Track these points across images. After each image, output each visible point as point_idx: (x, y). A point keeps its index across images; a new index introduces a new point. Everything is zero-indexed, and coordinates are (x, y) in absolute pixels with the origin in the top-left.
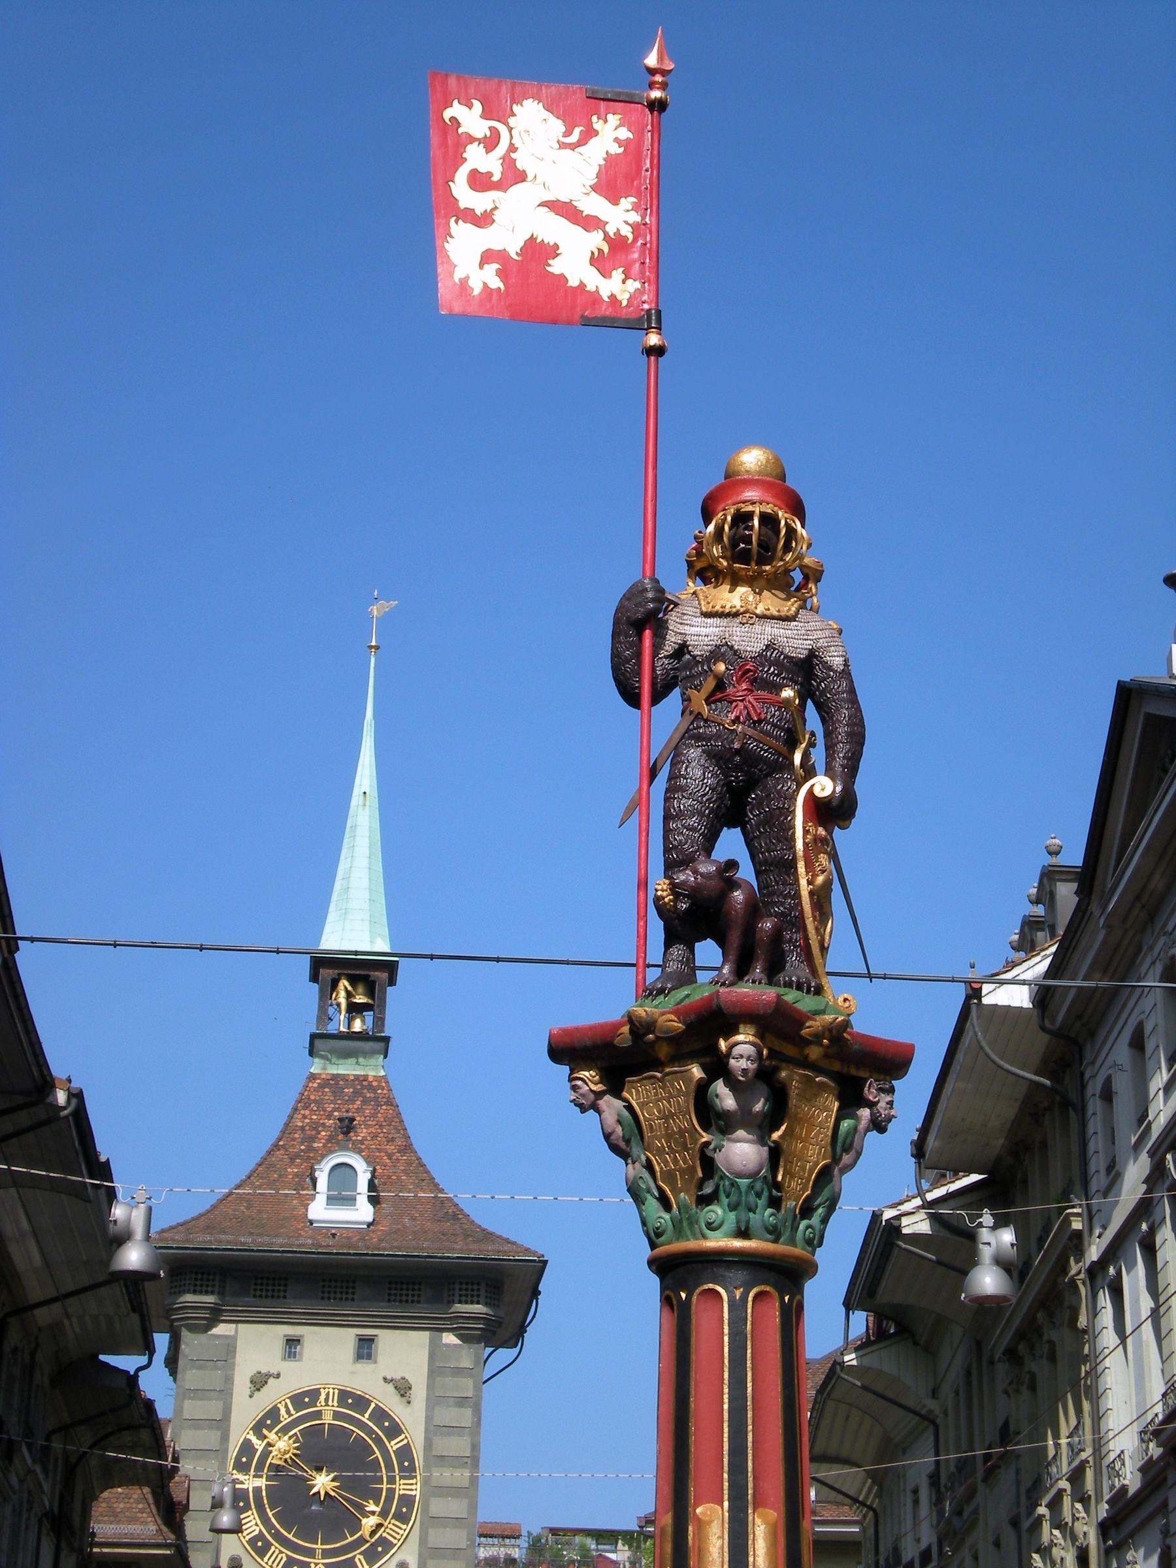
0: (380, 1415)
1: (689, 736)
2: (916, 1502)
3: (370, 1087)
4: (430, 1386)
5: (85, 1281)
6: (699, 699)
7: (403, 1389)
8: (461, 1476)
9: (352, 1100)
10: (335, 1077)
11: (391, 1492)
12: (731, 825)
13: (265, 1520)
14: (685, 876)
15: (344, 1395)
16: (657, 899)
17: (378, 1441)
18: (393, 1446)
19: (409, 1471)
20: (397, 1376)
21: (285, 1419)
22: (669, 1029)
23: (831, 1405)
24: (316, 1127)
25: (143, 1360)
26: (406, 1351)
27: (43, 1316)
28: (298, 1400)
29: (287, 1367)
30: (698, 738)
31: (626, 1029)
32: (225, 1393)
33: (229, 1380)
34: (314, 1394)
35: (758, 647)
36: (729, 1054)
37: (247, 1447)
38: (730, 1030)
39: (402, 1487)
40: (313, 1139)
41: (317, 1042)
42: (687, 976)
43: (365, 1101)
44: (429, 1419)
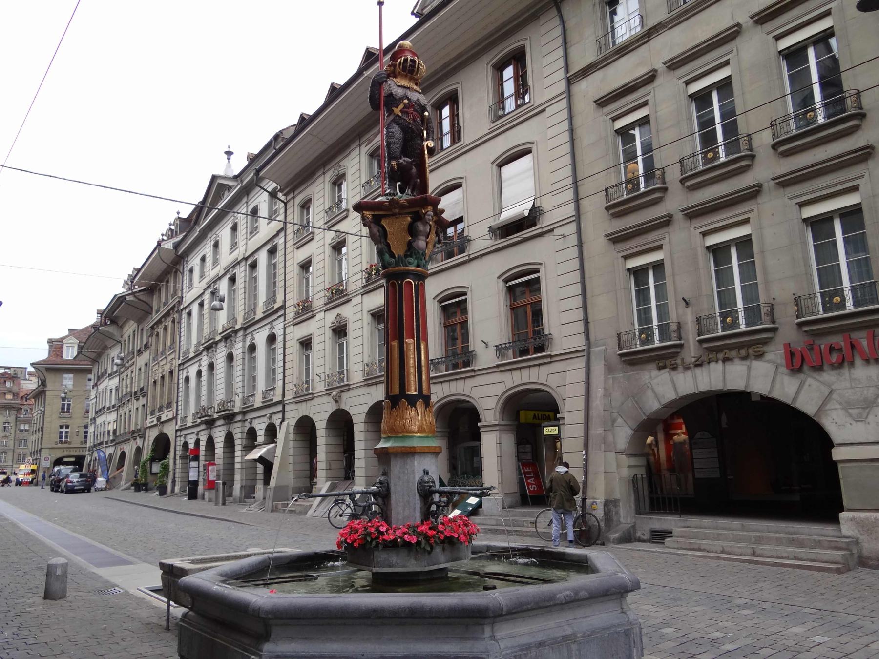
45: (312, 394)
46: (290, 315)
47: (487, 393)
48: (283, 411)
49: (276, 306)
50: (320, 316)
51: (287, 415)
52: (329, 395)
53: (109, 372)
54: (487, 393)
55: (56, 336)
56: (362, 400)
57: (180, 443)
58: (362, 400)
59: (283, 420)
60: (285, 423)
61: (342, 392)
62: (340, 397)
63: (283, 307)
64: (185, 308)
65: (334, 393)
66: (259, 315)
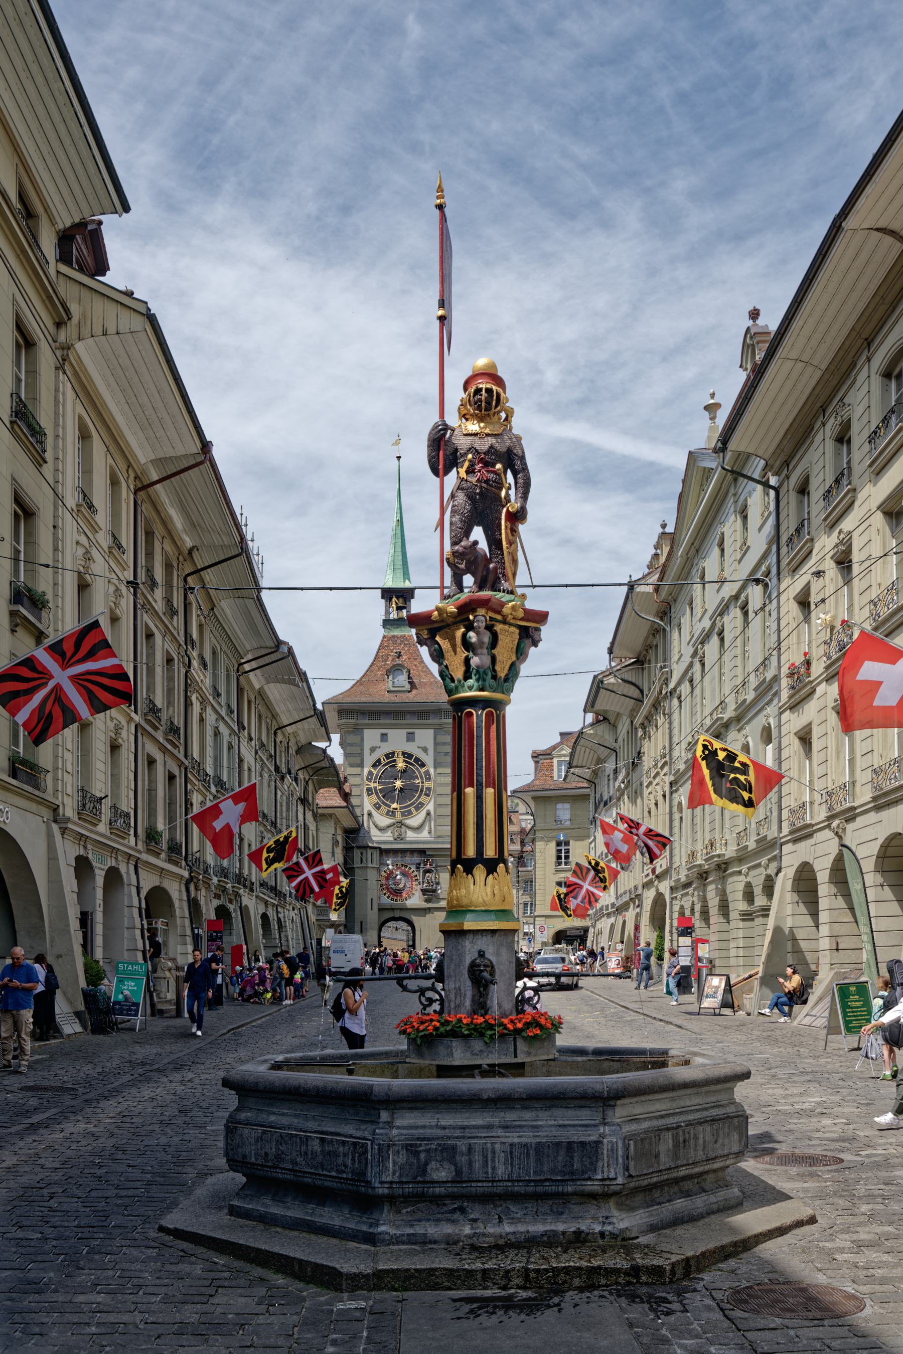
0: (417, 760)
2: (609, 780)
3: (407, 640)
4: (435, 750)
5: (303, 717)
6: (463, 474)
7: (425, 750)
9: (400, 645)
10: (393, 636)
11: (423, 786)
13: (379, 798)
14: (456, 548)
15: (404, 753)
16: (448, 559)
17: (417, 769)
18: (423, 770)
19: (429, 779)
20: (423, 745)
21: (383, 763)
22: (451, 613)
23: (578, 748)
24: (387, 656)
25: (328, 744)
27: (289, 729)
28: (387, 756)
29: (383, 744)
30: (462, 489)
31: (436, 613)
32: (361, 755)
33: (362, 750)
34: (393, 753)
36: (473, 621)
37: (370, 773)
38: (473, 611)
39: (426, 785)
40: (386, 660)
41: (387, 623)
42: (461, 588)
43: (405, 645)
44: (435, 760)
45: (812, 825)
46: (785, 695)
48: (779, 858)
49: (769, 675)
50: (820, 689)
51: (785, 861)
52: (829, 826)
53: (605, 798)
55: (543, 746)
56: (868, 834)
57: (676, 908)
58: (868, 834)
59: (779, 871)
60: (781, 875)
61: (848, 821)
62: (844, 830)
63: (776, 679)
64: (675, 689)
65: (835, 824)
66: (750, 696)
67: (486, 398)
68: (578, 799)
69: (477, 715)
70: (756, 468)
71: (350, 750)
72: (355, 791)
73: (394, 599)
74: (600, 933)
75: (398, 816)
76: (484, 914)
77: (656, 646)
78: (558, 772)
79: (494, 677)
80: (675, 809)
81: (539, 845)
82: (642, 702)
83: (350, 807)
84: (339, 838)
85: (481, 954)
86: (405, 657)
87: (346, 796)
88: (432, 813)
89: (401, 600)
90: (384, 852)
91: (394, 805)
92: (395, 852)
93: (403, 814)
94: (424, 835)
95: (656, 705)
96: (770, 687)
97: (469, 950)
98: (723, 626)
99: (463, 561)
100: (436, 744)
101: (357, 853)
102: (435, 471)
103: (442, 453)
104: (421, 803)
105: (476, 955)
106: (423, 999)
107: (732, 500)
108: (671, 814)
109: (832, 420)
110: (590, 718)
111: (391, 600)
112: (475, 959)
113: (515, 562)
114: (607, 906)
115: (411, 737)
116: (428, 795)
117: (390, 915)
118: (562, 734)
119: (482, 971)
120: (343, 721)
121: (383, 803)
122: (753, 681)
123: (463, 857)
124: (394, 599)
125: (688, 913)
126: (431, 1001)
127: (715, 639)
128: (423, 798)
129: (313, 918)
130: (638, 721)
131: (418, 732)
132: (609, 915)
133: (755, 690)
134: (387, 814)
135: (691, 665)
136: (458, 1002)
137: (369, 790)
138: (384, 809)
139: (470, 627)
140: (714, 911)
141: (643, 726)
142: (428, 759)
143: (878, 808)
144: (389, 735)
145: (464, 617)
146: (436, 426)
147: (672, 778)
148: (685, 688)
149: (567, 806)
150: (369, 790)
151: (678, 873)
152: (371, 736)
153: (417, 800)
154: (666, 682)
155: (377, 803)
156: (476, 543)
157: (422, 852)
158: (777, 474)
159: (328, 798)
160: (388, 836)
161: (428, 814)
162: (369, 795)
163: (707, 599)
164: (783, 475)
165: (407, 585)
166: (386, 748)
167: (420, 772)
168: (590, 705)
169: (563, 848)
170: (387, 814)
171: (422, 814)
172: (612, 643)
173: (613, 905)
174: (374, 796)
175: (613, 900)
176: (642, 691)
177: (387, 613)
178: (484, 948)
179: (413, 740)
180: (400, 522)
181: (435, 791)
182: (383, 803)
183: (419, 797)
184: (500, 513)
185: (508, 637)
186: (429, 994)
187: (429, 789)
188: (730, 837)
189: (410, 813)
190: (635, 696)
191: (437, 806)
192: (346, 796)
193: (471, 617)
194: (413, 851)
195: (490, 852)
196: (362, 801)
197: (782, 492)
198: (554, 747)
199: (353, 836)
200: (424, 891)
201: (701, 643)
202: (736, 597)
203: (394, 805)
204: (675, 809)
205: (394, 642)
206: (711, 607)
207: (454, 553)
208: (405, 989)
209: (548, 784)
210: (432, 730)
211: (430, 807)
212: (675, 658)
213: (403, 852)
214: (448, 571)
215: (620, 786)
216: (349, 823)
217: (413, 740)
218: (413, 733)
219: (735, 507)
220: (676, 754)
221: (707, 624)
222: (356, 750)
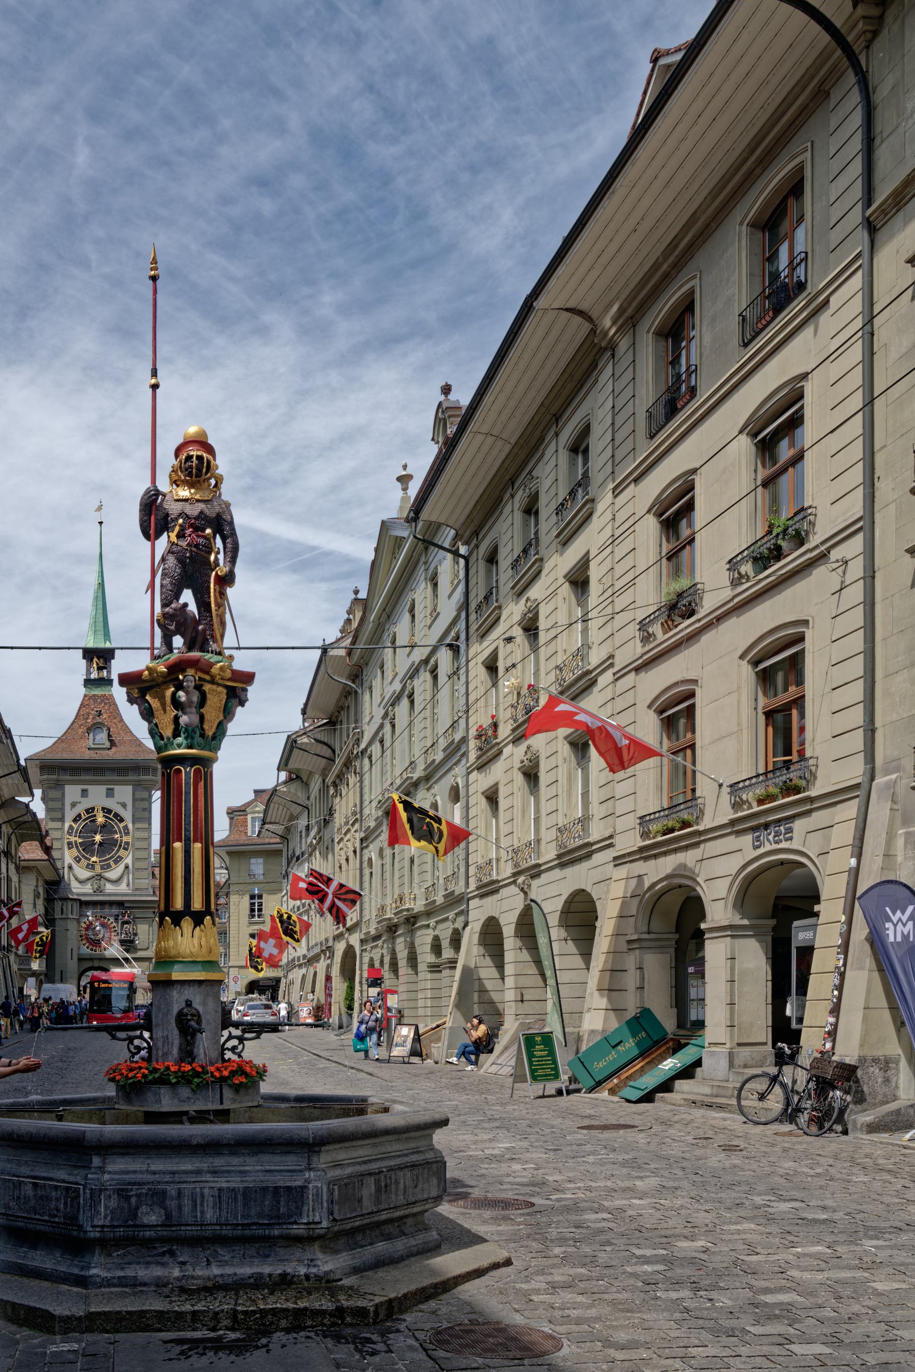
0: (116, 815)
1: (170, 552)
3: (107, 699)
5: (6, 772)
6: (174, 538)
7: (124, 805)
8: (146, 835)
9: (100, 704)
10: (94, 695)
12: (188, 588)
13: (79, 851)
14: (167, 610)
15: (103, 809)
16: (158, 620)
17: (116, 824)
18: (121, 825)
19: (127, 834)
21: (83, 817)
22: (161, 672)
23: (272, 805)
24: (88, 714)
25: (30, 799)
26: (124, 793)
28: (87, 811)
29: (83, 800)
30: (173, 553)
31: (146, 673)
32: (62, 810)
33: (63, 805)
34: (93, 809)
35: (196, 513)
36: (183, 681)
37: (71, 827)
38: (183, 671)
39: (125, 839)
40: (87, 718)
41: (88, 682)
42: (170, 649)
43: (105, 704)
44: (133, 816)
45: (497, 881)
46: (473, 755)
47: (719, 873)
48: (465, 913)
49: (458, 737)
50: (507, 751)
51: (472, 915)
52: (514, 882)
53: (298, 853)
54: (719, 873)
55: (238, 803)
56: (553, 890)
57: (366, 960)
58: (553, 890)
59: (466, 924)
60: (468, 929)
61: (533, 877)
62: (529, 886)
63: (464, 740)
64: (366, 749)
65: (521, 879)
66: (439, 757)
67: (196, 465)
68: (271, 854)
69: (186, 772)
70: (447, 537)
71: (52, 805)
72: (56, 845)
73: (95, 659)
74: (292, 983)
75: (98, 869)
76: (191, 965)
77: (348, 707)
78: (252, 829)
79: (202, 735)
80: (365, 864)
81: (234, 899)
82: (334, 761)
83: (51, 860)
84: (41, 890)
85: (189, 1004)
86: (105, 716)
87: (47, 850)
88: (131, 866)
89: (101, 660)
90: (84, 904)
91: (94, 859)
92: (94, 904)
93: (102, 868)
94: (123, 887)
95: (347, 764)
96: (458, 748)
97: (177, 1000)
98: (413, 689)
99: (172, 622)
100: (134, 800)
101: (58, 905)
102: (147, 535)
103: (153, 516)
104: (119, 857)
105: (184, 1005)
106: (132, 1048)
107: (423, 568)
108: (361, 869)
109: (521, 492)
110: (283, 776)
111: (92, 660)
112: (183, 1009)
113: (223, 624)
114: (299, 958)
115: (110, 793)
116: (126, 849)
117: (89, 964)
118: (257, 792)
119: (190, 1020)
120: (45, 777)
121: (83, 856)
122: (442, 743)
123: (171, 909)
124: (95, 659)
125: (377, 965)
126: (139, 1049)
127: (405, 702)
128: (122, 852)
129: (15, 967)
130: (330, 779)
131: (118, 789)
132: (300, 966)
133: (444, 750)
134: (87, 867)
135: (381, 726)
136: (165, 1050)
137: (69, 844)
138: (84, 862)
139: (179, 686)
140: (402, 963)
141: (335, 784)
142: (127, 815)
143: (562, 866)
144: (90, 792)
145: (174, 677)
146: (148, 492)
147: (363, 835)
148: (376, 749)
149: (261, 860)
150: (69, 844)
151: (368, 927)
152: (72, 792)
153: (116, 854)
154: (358, 742)
155: (78, 856)
156: (186, 605)
157: (120, 904)
158: (467, 543)
159: (30, 851)
160: (88, 888)
161: (127, 867)
162: (69, 848)
163: (397, 663)
164: (473, 545)
165: (108, 645)
166: (86, 803)
167: (119, 827)
168: (284, 764)
169: (256, 901)
170: (87, 867)
171: (121, 867)
172: (306, 705)
173: (304, 956)
174: (74, 850)
175: (305, 951)
176: (334, 751)
177: (89, 672)
178: (191, 998)
179: (113, 796)
180: (102, 585)
181: (133, 845)
182: (83, 856)
183: (118, 851)
184: (210, 577)
185: (216, 697)
186: (137, 1042)
187: (127, 843)
188: (419, 891)
189: (109, 866)
190: (327, 755)
191: (135, 859)
192: (47, 850)
193: (181, 677)
194: (111, 904)
195: (197, 904)
196: (63, 854)
197: (472, 560)
198: (248, 804)
199: (53, 888)
200: (122, 942)
201: (391, 705)
202: (426, 661)
203: (94, 859)
204: (365, 864)
205: (95, 701)
206: (402, 669)
207: (165, 615)
208: (114, 1037)
209: (242, 839)
210: (131, 787)
211: (129, 860)
212: (366, 719)
213: (102, 904)
214: (158, 631)
215: (312, 842)
216: (50, 876)
217: (113, 796)
218: (112, 789)
219: (426, 575)
220: (366, 812)
221: (397, 686)
222: (58, 805)
